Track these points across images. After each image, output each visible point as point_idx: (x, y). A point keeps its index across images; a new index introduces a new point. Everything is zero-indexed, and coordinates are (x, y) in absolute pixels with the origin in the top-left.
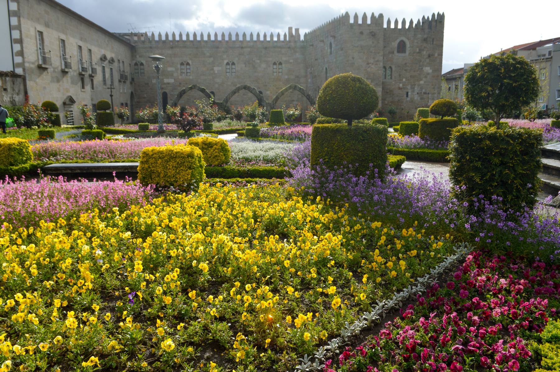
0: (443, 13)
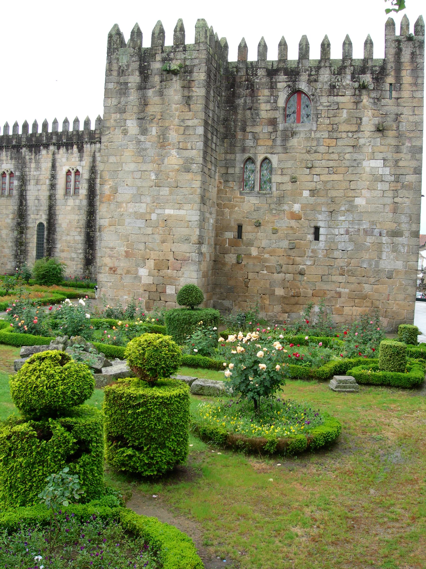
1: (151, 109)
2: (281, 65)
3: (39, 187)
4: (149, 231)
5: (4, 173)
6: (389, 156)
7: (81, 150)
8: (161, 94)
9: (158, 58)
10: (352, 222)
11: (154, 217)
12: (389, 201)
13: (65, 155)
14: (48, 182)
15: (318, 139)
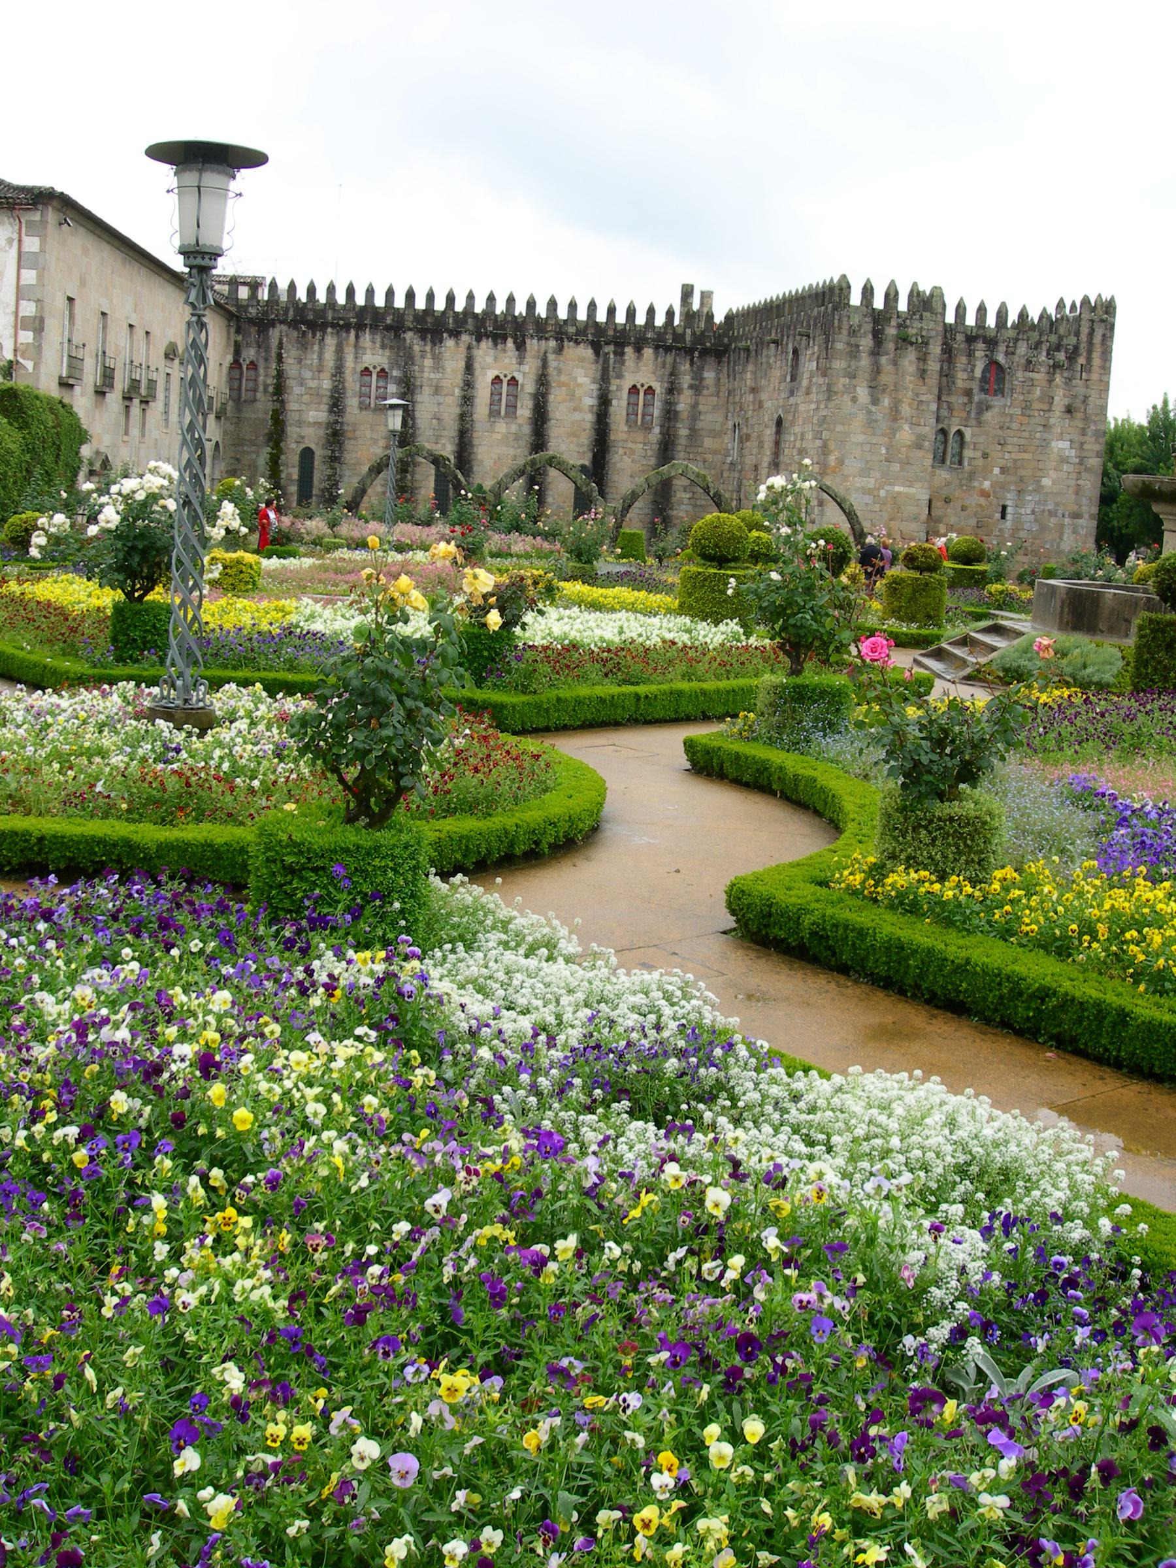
0: (1112, 298)
1: (886, 378)
2: (981, 332)
3: (440, 399)
4: (877, 507)
5: (367, 369)
6: (1076, 437)
7: (520, 346)
8: (895, 363)
9: (894, 323)
10: (1038, 503)
11: (882, 493)
12: (1073, 483)
13: (492, 352)
14: (457, 392)
15: (1011, 416)
